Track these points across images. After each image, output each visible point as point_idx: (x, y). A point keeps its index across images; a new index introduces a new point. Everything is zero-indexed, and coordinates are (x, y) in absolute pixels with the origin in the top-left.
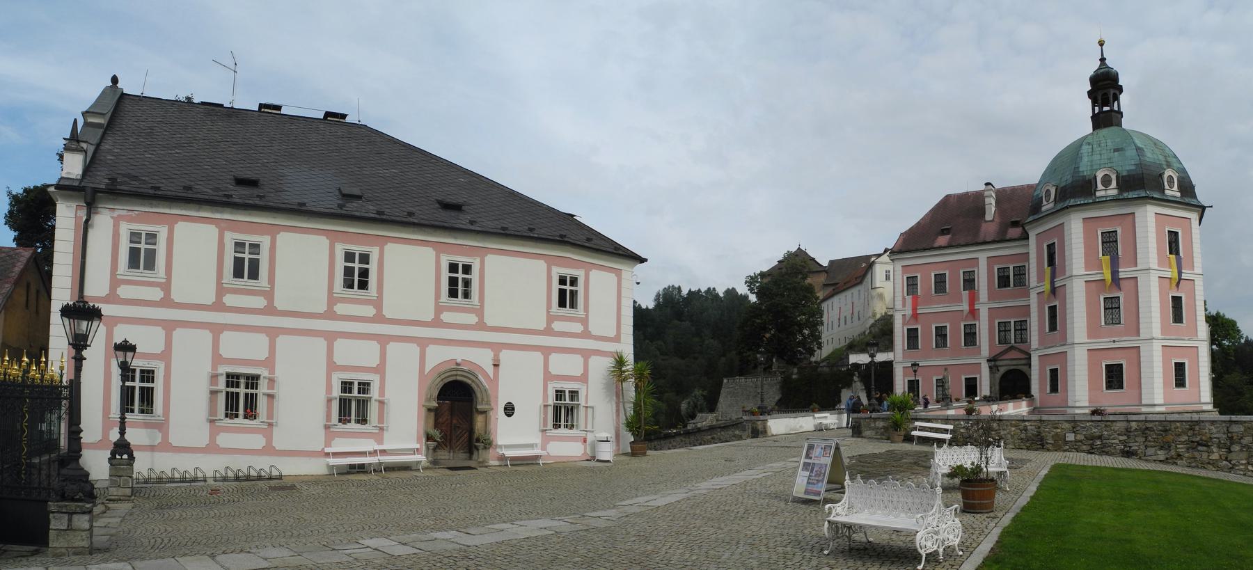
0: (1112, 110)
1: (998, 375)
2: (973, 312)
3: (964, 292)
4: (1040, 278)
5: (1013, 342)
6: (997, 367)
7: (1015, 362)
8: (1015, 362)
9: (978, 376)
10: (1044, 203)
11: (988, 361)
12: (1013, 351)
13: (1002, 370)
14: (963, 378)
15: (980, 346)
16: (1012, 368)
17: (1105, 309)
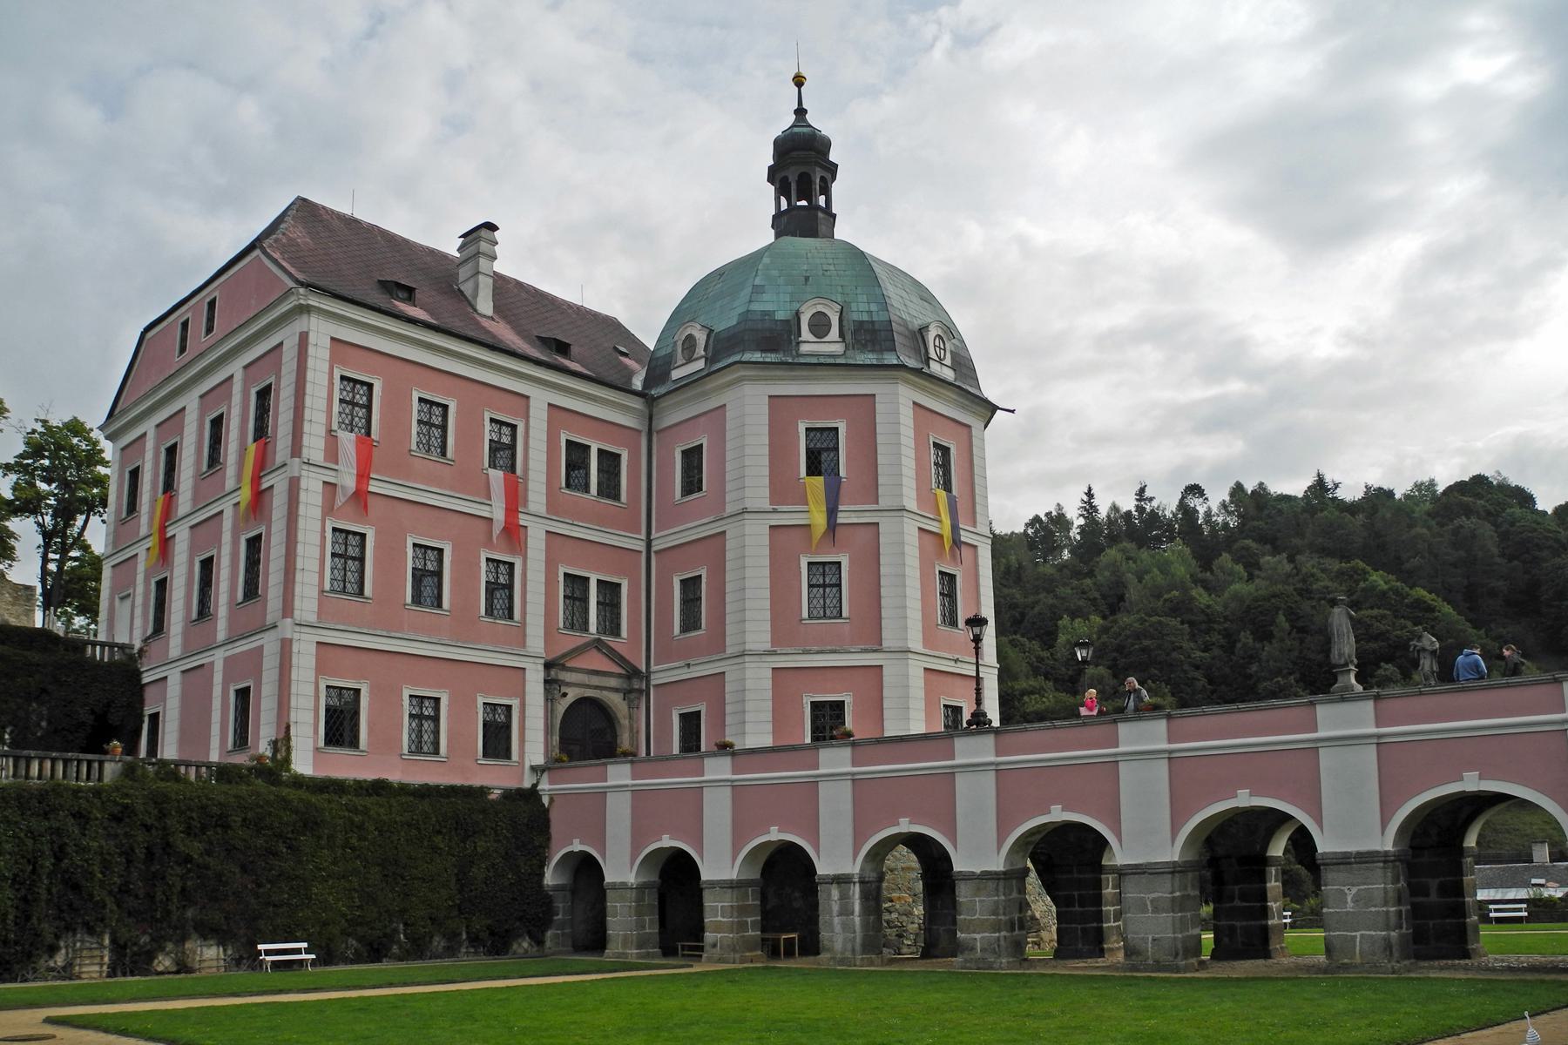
0: (813, 207)
1: (562, 706)
2: (513, 533)
3: (492, 472)
4: (783, 490)
5: (593, 628)
6: (560, 683)
7: (595, 680)
8: (595, 680)
9: (515, 703)
10: (806, 334)
11: (548, 666)
12: (594, 653)
13: (573, 694)
14: (480, 701)
15: (524, 623)
16: (590, 693)
17: (810, 586)
